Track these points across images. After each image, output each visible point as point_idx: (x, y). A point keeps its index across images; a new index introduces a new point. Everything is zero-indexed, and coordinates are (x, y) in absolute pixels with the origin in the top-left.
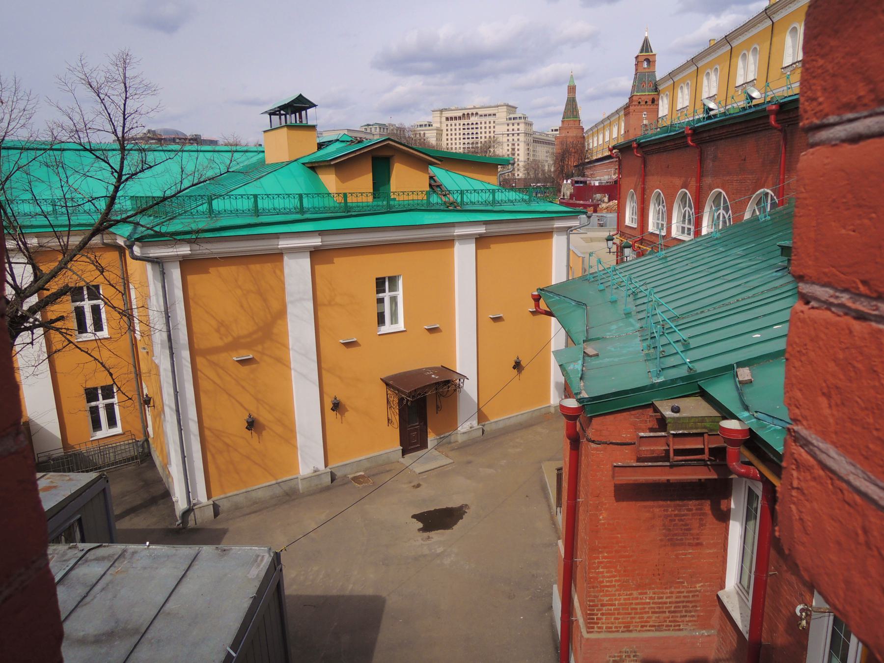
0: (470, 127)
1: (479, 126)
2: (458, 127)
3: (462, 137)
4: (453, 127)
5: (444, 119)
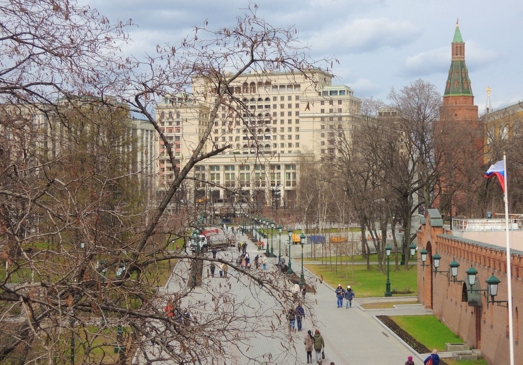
1: (271, 103)
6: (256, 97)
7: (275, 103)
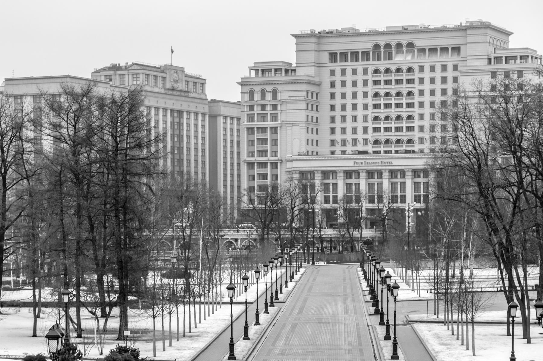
0: (393, 77)
1: (416, 76)
2: (360, 78)
3: (370, 101)
4: (349, 78)
5: (326, 57)
6: (393, 68)
7: (421, 75)
